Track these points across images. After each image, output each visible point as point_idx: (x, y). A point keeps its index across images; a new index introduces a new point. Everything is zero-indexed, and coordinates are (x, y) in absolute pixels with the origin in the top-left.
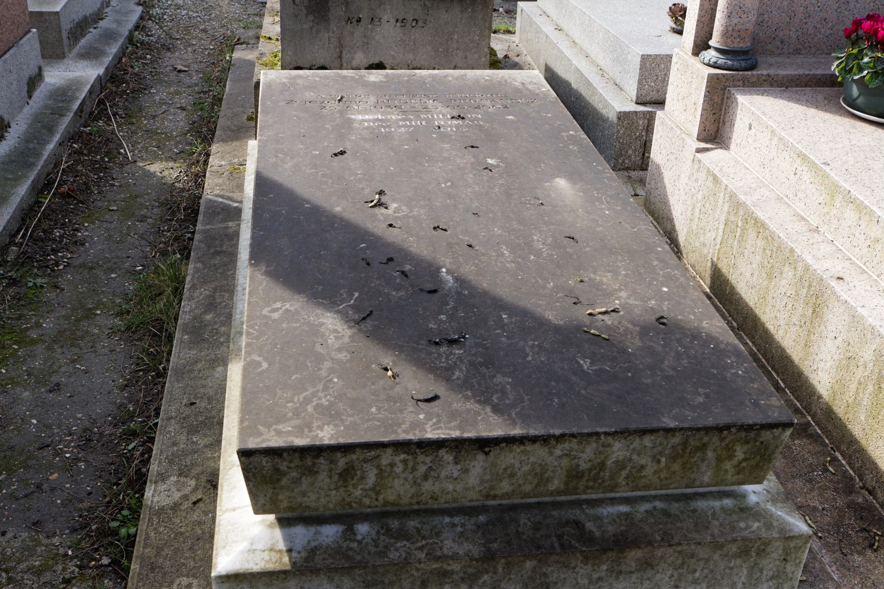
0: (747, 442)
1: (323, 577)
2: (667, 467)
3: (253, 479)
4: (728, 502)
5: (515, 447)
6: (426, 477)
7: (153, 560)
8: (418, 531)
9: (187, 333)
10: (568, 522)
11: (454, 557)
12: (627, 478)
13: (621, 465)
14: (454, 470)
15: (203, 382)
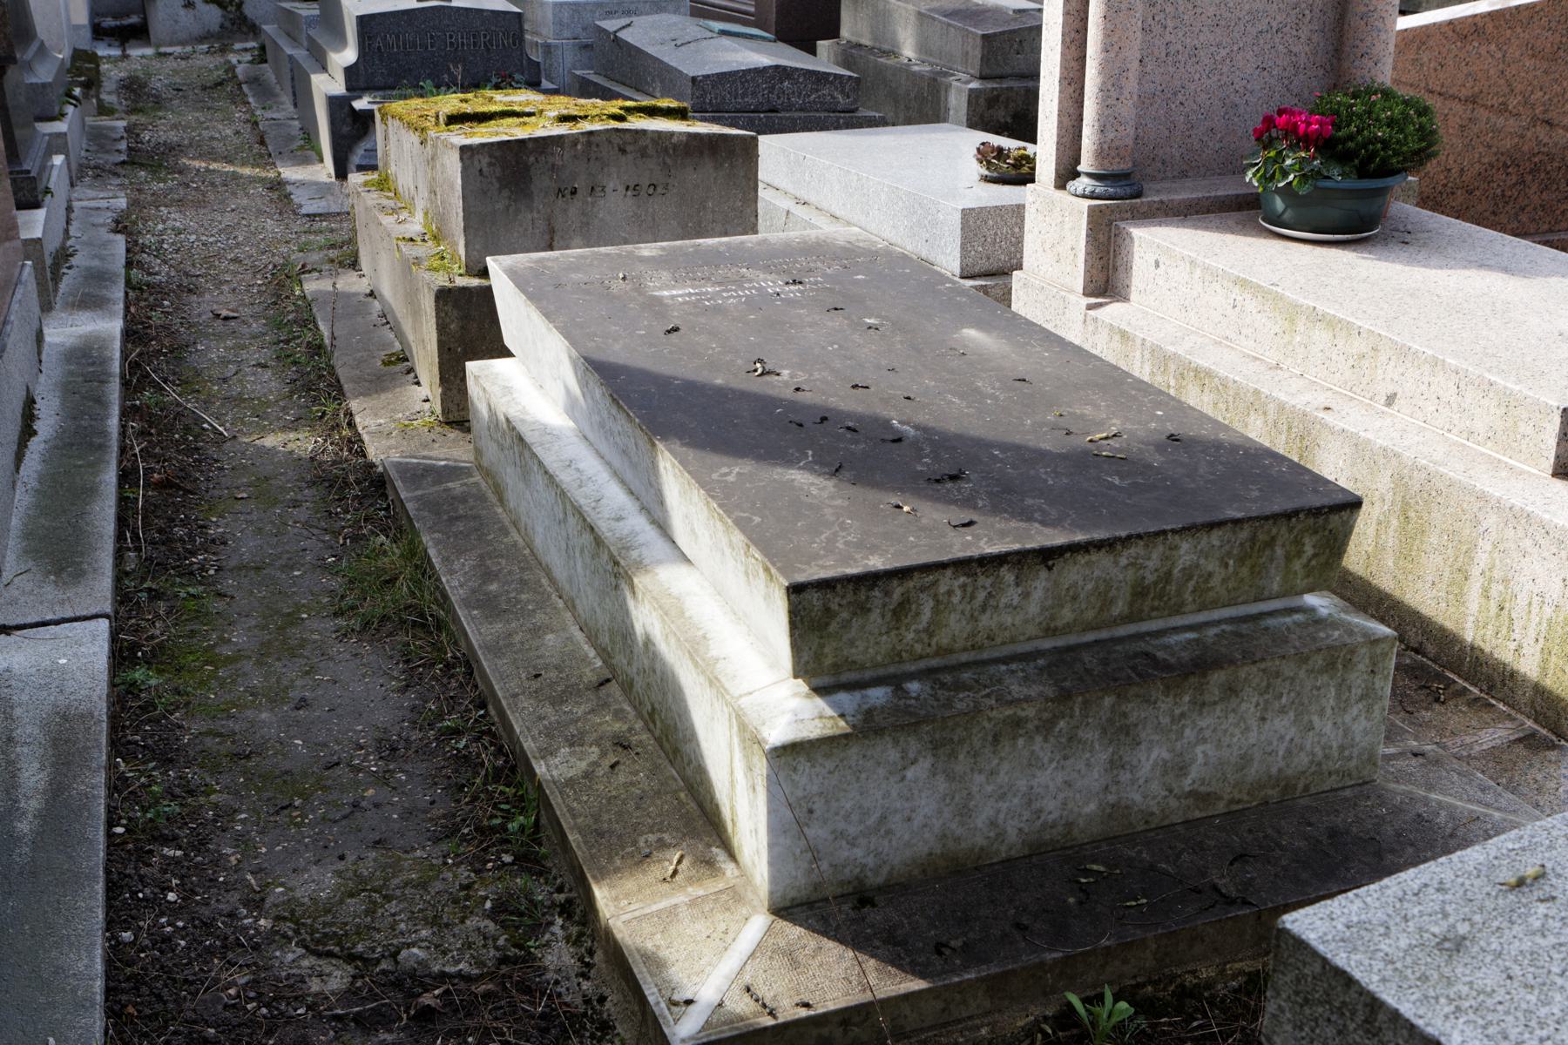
0: (1316, 532)
1: (888, 738)
2: (1236, 573)
3: (800, 626)
4: (1298, 617)
5: (1080, 557)
6: (984, 609)
7: (594, 827)
8: (977, 681)
9: (474, 608)
10: (1136, 655)
11: (1028, 699)
12: (1193, 592)
13: (1188, 573)
14: (1012, 595)
15: (539, 653)
